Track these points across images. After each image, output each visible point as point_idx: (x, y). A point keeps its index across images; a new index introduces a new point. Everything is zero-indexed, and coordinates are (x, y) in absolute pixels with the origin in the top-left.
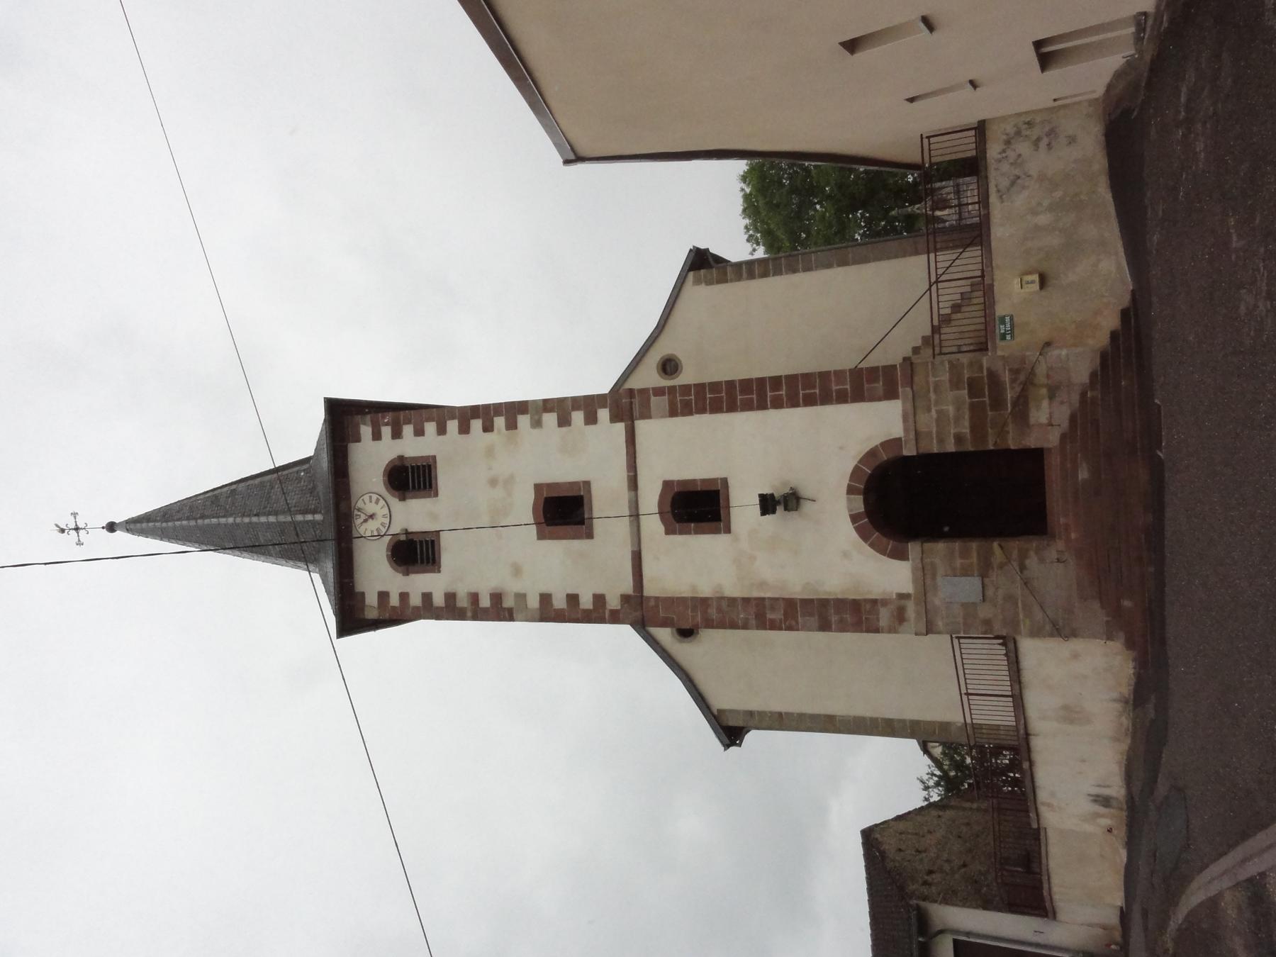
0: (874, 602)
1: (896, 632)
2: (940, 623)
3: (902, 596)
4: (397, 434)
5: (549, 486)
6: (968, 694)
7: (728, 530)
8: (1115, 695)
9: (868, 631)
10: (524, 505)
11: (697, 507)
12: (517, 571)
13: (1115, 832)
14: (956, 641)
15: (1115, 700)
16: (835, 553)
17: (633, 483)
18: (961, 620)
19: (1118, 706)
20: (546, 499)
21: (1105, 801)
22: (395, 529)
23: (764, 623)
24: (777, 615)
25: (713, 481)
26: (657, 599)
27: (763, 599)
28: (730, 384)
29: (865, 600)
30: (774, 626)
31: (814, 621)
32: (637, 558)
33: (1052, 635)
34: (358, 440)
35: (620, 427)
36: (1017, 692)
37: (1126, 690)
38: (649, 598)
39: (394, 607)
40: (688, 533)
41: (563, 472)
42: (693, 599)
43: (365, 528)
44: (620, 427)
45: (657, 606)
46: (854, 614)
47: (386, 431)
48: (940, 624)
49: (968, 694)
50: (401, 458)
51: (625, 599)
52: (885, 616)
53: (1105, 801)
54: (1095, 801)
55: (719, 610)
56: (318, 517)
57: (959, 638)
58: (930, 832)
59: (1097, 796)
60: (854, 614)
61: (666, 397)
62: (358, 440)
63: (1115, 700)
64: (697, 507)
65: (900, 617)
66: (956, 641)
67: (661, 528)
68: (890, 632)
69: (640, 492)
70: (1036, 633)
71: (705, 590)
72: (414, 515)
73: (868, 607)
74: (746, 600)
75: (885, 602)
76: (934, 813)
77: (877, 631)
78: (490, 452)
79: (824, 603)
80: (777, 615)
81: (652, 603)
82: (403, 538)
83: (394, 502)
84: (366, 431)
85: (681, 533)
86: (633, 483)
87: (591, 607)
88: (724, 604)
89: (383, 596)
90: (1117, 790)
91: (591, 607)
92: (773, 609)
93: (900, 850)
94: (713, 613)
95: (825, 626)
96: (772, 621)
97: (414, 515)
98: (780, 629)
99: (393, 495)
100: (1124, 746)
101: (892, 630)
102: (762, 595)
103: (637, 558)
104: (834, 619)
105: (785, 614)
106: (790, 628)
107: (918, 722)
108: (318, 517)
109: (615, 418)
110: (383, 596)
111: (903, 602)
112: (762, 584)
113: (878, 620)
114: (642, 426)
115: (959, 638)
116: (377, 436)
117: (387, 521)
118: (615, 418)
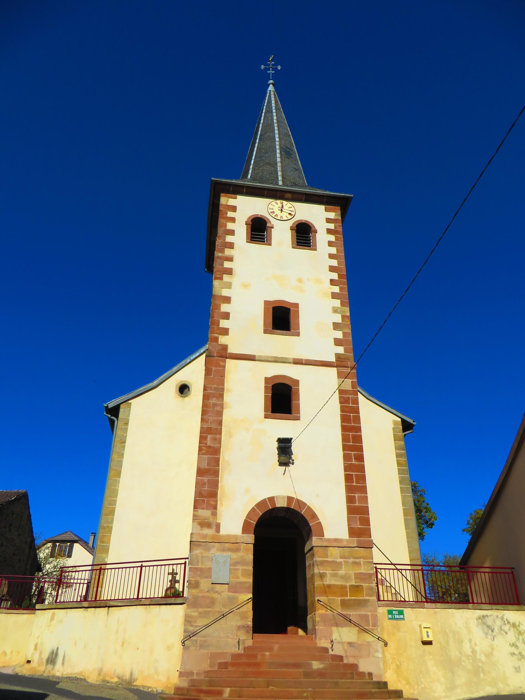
0: (215, 508)
1: (194, 520)
2: (198, 551)
3: (218, 526)
4: (329, 231)
5: (297, 312)
6: (142, 567)
7: (266, 417)
8: (136, 675)
9: (196, 501)
10: (287, 296)
11: (282, 399)
12: (246, 286)
13: (28, 666)
14: (183, 561)
15: (131, 674)
16: (251, 484)
17: (297, 362)
18: (200, 566)
19: (127, 676)
20: (289, 309)
21: (52, 659)
22: (273, 222)
23: (204, 433)
24: (209, 442)
25: (298, 412)
26: (224, 367)
27: (221, 434)
28: (359, 429)
29: (216, 501)
30: (202, 439)
31: (204, 465)
32: (251, 358)
33: (185, 631)
34: (326, 210)
35: (333, 359)
36: (144, 602)
37: (139, 683)
38: (225, 362)
39: (227, 213)
40: (266, 392)
41: (305, 319)
42: (223, 389)
43: (275, 205)
44: (333, 359)
45: (220, 366)
46: (207, 493)
47: (332, 226)
48: (197, 551)
49: (142, 567)
50: (316, 232)
51: (225, 347)
52: (205, 513)
53: (52, 659)
54: (53, 652)
55: (215, 405)
56: (280, 183)
57: (185, 563)
58: (19, 535)
59: (57, 654)
60: (207, 493)
61: (351, 389)
62: (326, 210)
63: (131, 674)
64: (282, 399)
65: (204, 524)
66: (183, 561)
67: (269, 376)
68: (194, 516)
69: (292, 365)
70: (188, 620)
71: (227, 398)
72: (282, 233)
73: (212, 503)
74: (220, 423)
75: (214, 514)
76: (29, 540)
77: (195, 507)
78: (318, 281)
79: (216, 473)
80: (209, 442)
81: (222, 364)
82: (268, 225)
83: (290, 223)
84: (332, 215)
85: (265, 387)
86: (297, 362)
87: (220, 326)
88: (218, 408)
89: (234, 209)
90: (59, 670)
91: (220, 326)
92: (215, 439)
93: (13, 514)
94: (213, 401)
95: (200, 472)
96: (206, 438)
97: (282, 233)
98: (200, 443)
99: (293, 224)
100: (93, 679)
101: (195, 518)
102: (223, 433)
103: (251, 358)
104: (205, 479)
105: (210, 447)
106: (200, 449)
107: (110, 532)
108: (280, 183)
109: (338, 356)
110: (234, 209)
111: (214, 527)
112: (230, 435)
113: (203, 509)
114: (334, 371)
115: (185, 563)
116: (329, 220)
117: (279, 218)
118: (338, 356)
